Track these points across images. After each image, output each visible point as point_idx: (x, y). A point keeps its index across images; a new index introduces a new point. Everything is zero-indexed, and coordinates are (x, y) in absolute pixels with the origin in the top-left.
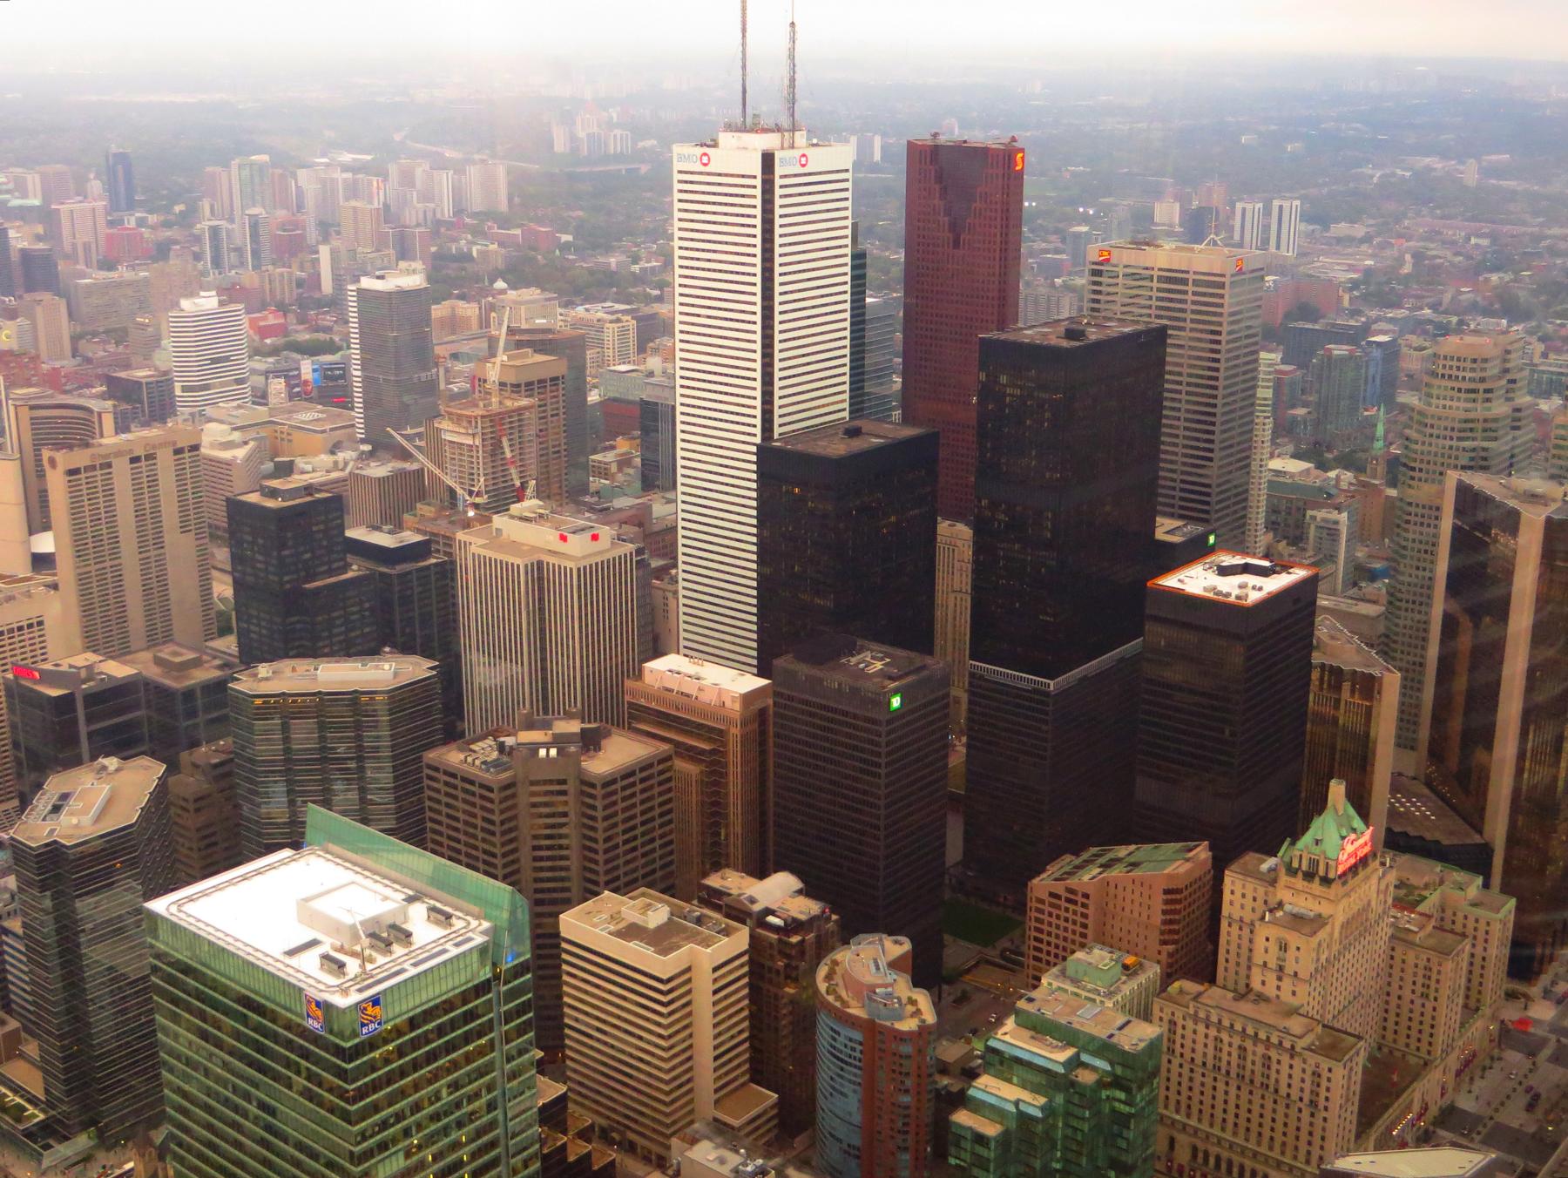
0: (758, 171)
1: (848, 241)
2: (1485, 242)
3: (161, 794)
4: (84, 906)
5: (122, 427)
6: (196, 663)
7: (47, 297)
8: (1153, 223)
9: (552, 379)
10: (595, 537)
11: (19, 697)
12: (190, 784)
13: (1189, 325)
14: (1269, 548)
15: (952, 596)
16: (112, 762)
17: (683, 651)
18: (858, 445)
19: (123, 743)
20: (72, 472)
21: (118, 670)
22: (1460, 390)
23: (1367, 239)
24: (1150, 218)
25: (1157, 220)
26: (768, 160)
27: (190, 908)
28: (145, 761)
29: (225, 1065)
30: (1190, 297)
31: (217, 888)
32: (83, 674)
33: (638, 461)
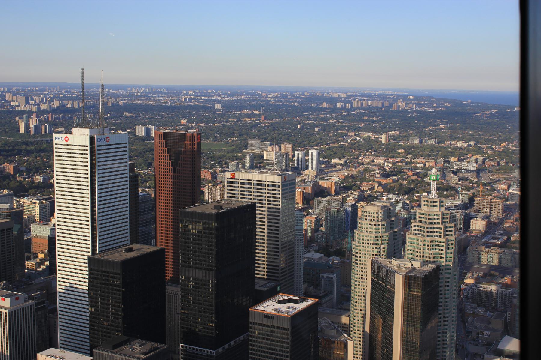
0: (88, 144)
1: (127, 171)
2: (390, 165)
8: (263, 159)
9: (7, 229)
10: (17, 299)
13: (266, 202)
14: (306, 289)
15: (177, 316)
17: (59, 345)
18: (130, 255)
22: (372, 225)
23: (346, 164)
24: (262, 157)
25: (265, 158)
26: (92, 139)
30: (266, 191)
33: (47, 263)
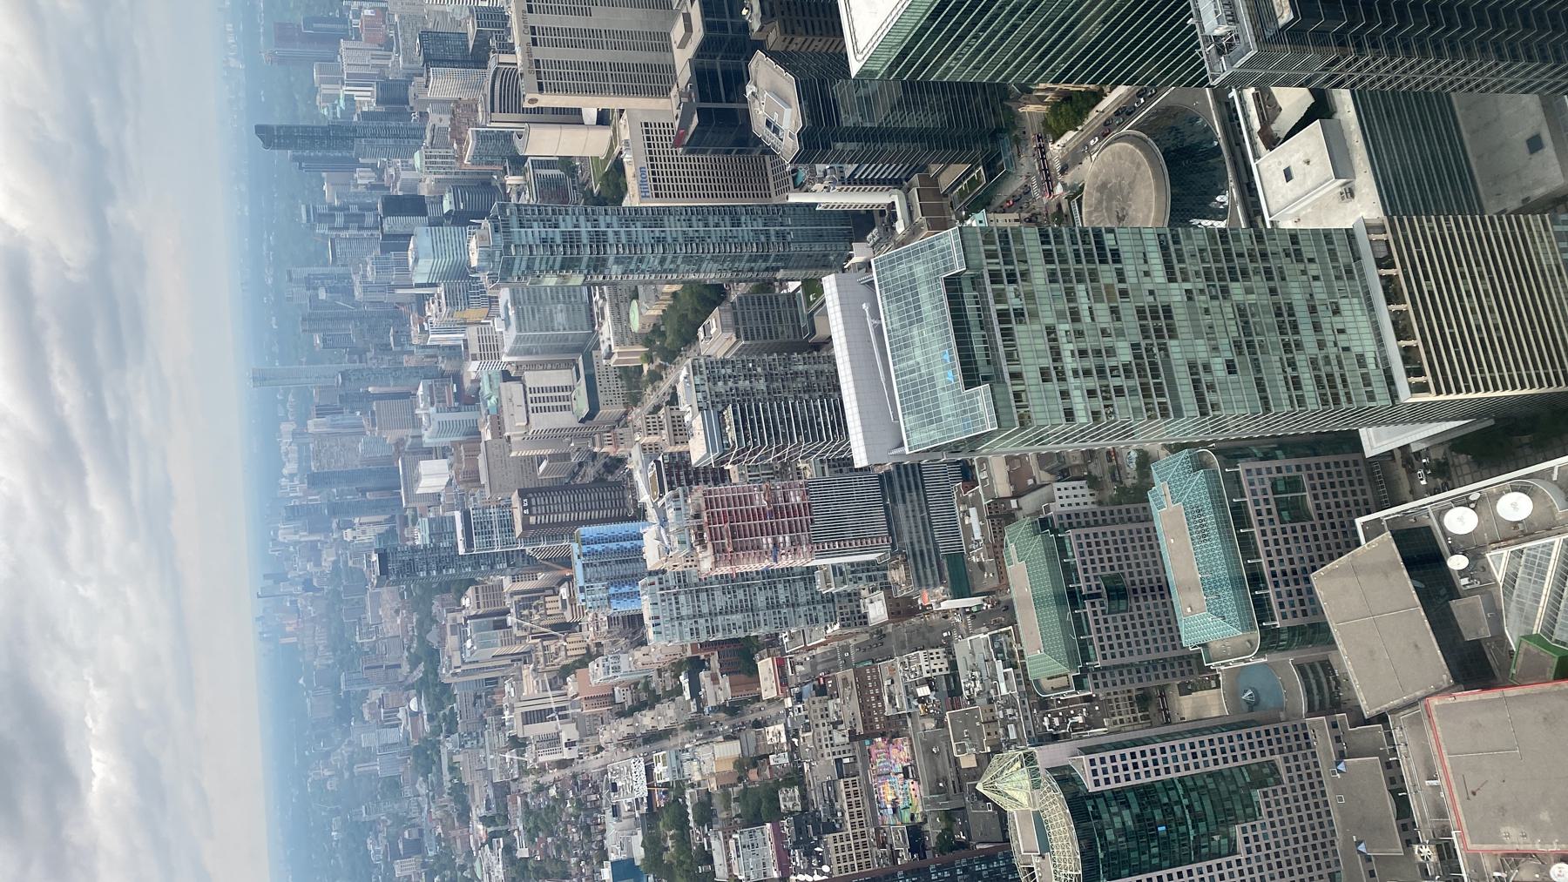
3: (779, 58)
4: (849, 120)
5: (510, 49)
6: (687, 18)
7: (412, 91)
11: (696, 145)
12: (773, 37)
16: (750, 89)
19: (738, 78)
20: (540, 85)
21: (684, 73)
27: (861, 46)
28: (752, 65)
29: (976, 37)
31: (851, 24)
32: (685, 100)
